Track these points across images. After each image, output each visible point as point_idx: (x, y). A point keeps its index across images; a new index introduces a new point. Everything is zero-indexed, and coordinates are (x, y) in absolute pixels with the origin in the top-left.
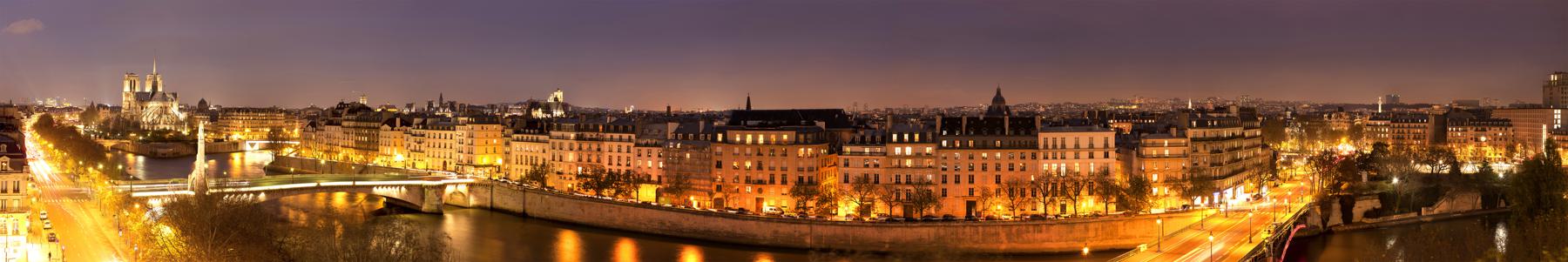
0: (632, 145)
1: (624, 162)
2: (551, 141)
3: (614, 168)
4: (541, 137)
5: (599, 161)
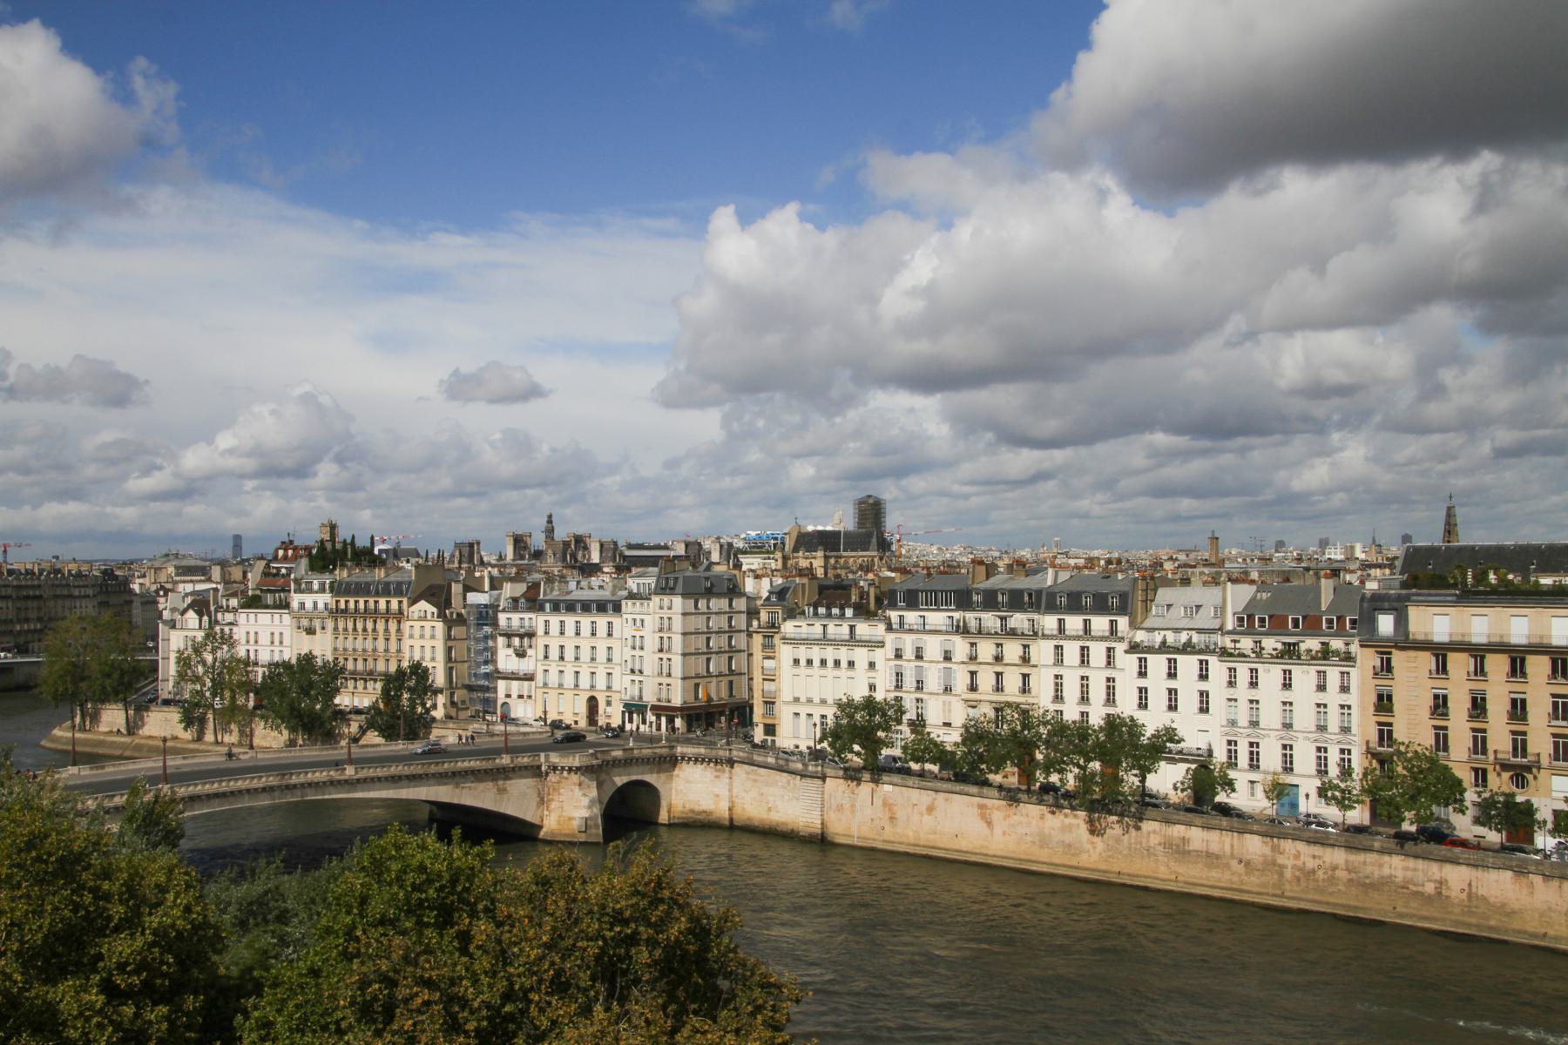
0: (1120, 647)
1: (1098, 692)
2: (890, 638)
3: (1071, 713)
4: (864, 629)
5: (1025, 690)
